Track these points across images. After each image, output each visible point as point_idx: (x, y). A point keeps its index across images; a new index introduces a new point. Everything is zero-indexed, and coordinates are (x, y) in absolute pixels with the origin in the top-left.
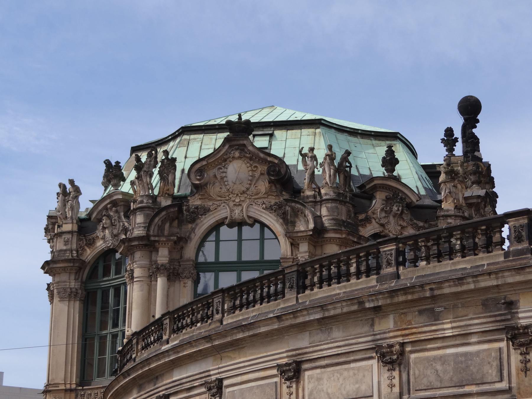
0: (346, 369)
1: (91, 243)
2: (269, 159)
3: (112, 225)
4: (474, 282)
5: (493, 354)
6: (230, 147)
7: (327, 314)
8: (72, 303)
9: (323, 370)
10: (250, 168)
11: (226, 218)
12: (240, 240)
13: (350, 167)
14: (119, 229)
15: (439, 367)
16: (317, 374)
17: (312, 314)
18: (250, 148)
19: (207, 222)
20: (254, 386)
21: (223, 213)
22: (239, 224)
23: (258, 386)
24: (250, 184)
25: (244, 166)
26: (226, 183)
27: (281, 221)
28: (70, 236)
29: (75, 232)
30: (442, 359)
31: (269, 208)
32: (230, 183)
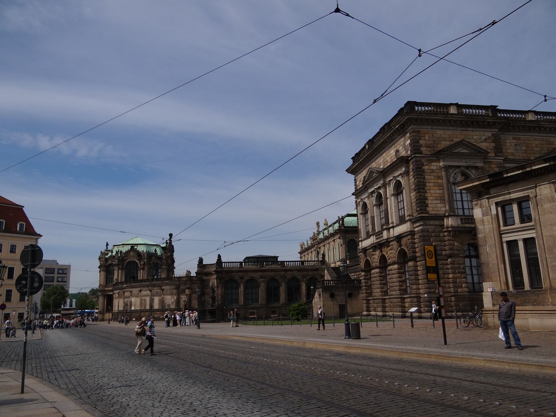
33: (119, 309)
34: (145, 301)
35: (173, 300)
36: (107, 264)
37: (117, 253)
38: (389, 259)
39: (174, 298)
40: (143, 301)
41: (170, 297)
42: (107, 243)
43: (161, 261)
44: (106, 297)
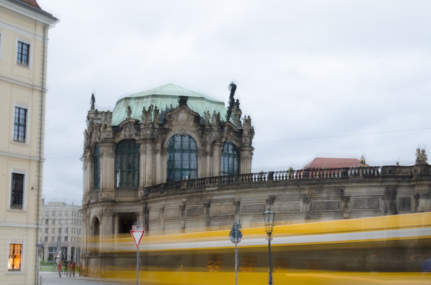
0: (291, 203)
3: (129, 131)
4: (334, 185)
5: (337, 202)
6: (180, 108)
7: (286, 188)
8: (111, 159)
9: (282, 202)
11: (178, 134)
13: (220, 118)
14: (133, 132)
15: (321, 205)
16: (280, 203)
17: (281, 187)
20: (254, 205)
23: (256, 205)
24: (187, 122)
25: (185, 116)
26: (178, 121)
28: (109, 133)
29: (111, 131)
30: (323, 202)
32: (180, 121)
36: (117, 140)
37: (146, 113)
38: (408, 173)
42: (93, 96)
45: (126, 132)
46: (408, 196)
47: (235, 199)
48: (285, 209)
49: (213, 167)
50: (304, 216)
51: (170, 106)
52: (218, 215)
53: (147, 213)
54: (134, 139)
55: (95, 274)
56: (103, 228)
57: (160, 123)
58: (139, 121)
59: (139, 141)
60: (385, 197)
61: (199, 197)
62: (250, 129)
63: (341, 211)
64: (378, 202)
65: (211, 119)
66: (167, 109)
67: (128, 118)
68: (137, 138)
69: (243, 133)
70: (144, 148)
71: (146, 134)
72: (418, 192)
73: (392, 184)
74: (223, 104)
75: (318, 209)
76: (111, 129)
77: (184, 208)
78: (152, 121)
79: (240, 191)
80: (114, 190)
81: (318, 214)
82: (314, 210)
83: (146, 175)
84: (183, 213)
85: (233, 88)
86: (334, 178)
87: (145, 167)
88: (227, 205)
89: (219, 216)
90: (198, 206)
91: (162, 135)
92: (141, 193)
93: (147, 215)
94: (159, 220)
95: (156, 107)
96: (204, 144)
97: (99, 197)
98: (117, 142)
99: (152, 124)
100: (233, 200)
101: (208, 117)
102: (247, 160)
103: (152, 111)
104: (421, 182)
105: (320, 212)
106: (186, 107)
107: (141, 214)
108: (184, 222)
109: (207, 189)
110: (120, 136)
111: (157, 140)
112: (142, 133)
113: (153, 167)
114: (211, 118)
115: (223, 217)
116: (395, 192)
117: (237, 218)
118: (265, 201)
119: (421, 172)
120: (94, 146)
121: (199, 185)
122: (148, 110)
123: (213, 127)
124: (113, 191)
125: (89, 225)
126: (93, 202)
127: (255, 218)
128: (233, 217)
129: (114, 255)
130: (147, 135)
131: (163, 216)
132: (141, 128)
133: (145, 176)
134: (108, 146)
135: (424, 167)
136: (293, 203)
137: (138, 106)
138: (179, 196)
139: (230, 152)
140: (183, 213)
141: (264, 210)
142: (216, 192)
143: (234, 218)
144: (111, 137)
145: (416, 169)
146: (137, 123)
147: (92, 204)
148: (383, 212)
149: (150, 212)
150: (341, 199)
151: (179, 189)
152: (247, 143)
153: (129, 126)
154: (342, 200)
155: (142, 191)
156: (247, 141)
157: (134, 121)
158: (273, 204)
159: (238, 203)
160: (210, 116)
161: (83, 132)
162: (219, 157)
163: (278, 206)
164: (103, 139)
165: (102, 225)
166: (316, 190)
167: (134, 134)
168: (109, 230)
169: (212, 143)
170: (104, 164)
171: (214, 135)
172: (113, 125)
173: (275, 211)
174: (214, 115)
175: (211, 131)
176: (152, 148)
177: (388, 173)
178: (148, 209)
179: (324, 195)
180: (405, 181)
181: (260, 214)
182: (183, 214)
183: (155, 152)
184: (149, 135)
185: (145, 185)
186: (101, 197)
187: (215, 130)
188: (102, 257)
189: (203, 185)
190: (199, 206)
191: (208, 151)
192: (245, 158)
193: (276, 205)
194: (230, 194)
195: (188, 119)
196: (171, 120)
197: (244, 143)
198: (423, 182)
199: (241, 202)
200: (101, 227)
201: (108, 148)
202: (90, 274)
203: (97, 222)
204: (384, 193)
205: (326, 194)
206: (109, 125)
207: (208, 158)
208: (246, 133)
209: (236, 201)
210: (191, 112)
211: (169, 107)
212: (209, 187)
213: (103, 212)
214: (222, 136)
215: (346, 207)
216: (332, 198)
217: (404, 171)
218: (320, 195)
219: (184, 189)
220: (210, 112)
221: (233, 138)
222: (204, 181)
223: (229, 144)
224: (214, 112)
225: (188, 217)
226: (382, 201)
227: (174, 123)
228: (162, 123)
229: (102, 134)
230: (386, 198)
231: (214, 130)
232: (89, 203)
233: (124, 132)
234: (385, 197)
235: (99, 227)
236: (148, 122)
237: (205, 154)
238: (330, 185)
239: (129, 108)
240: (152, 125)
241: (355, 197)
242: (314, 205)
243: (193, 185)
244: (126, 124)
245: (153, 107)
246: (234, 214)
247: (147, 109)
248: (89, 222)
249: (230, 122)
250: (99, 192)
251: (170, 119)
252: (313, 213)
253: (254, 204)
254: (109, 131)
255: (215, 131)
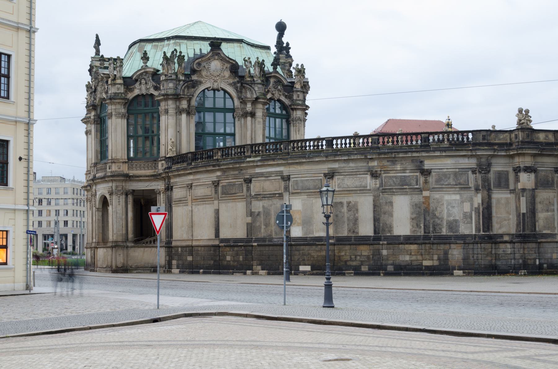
0: (355, 177)
1: (131, 90)
2: (231, 61)
3: (146, 83)
6: (212, 53)
7: (350, 158)
8: (123, 120)
9: (345, 176)
10: (222, 65)
11: (210, 87)
12: (214, 97)
13: (264, 67)
15: (394, 180)
18: (222, 55)
19: (202, 88)
21: (208, 85)
22: (214, 90)
23: (311, 180)
25: (219, 63)
27: (235, 91)
28: (120, 86)
29: (122, 84)
30: (396, 177)
31: (230, 84)
32: (212, 71)
33: (222, 236)
34: (353, 208)
35: (467, 207)
36: (130, 96)
37: (167, 60)
38: (506, 140)
39: (471, 200)
40: (345, 209)
41: (458, 197)
42: (97, 37)
43: (290, 97)
44: (130, 198)
45: (142, 85)
46: (505, 169)
47: (284, 172)
48: (347, 185)
49: (255, 130)
50: (372, 194)
51: (199, 51)
52: (261, 193)
53: (171, 191)
54: (152, 95)
55: (104, 268)
56: (114, 210)
57: (186, 73)
58: (158, 71)
59: (158, 97)
60: (477, 170)
61: (237, 170)
62: (304, 82)
63: (420, 188)
64: (468, 177)
65: (253, 68)
66: (194, 54)
67: (144, 67)
68: (156, 93)
69: (295, 86)
70: (165, 106)
71: (168, 88)
72: (518, 163)
73: (485, 153)
74: (268, 48)
75: (390, 186)
76: (122, 80)
77: (218, 184)
78: (176, 71)
79: (290, 162)
80: (127, 160)
81: (391, 192)
82: (385, 186)
83: (168, 142)
84: (216, 190)
85: (281, 28)
86: (412, 145)
87: (166, 130)
88: (273, 181)
89: (262, 195)
90: (236, 182)
91: (188, 89)
92: (162, 164)
93: (170, 193)
94: (186, 199)
95: (181, 52)
96: (243, 102)
97: (108, 170)
98: (131, 98)
99: (176, 74)
100: (280, 173)
101: (249, 65)
102: (299, 121)
103: (176, 58)
104: (523, 151)
105: (392, 189)
106: (220, 52)
107: (163, 191)
108: (219, 202)
109: (248, 159)
110: (133, 90)
111: (182, 96)
112: (163, 86)
113: (178, 131)
114: (252, 67)
115: (268, 196)
116: (489, 163)
117: (286, 196)
118: (322, 175)
119: (523, 139)
120: (100, 104)
121: (238, 154)
122: (170, 57)
123: (255, 79)
124: (126, 162)
125: (95, 206)
126: (99, 176)
127: (309, 196)
128: (281, 196)
129: (128, 245)
130: (169, 89)
131: (191, 194)
132: (161, 79)
133: (168, 143)
134: (119, 103)
135: (527, 132)
136: (359, 177)
137: (158, 50)
138: (211, 168)
139: (277, 112)
140: (216, 190)
141: (320, 187)
142: (259, 164)
143: (283, 197)
144: (122, 91)
145: (517, 135)
146: (155, 74)
147: (98, 179)
148: (473, 189)
149: (174, 190)
150: (420, 172)
151: (212, 159)
152: (300, 100)
153: (145, 77)
154: (421, 174)
155: (163, 162)
156: (300, 97)
157: (152, 70)
158: (332, 178)
159: (288, 178)
160: (251, 64)
161: (85, 85)
162: (263, 118)
163: (339, 182)
164: (112, 94)
165: (112, 205)
166: (388, 161)
167: (152, 88)
168: (121, 212)
169: (254, 99)
170: (113, 127)
171: (256, 89)
172: (125, 76)
173: (335, 187)
174: (257, 63)
175: (252, 84)
176: (177, 106)
177: (481, 139)
178: (171, 185)
179: (398, 167)
180: (503, 150)
181: (315, 192)
182: (216, 192)
183: (179, 112)
184: (171, 89)
185: (166, 154)
186: (110, 170)
187: (258, 82)
188: (112, 247)
189: (242, 154)
190: (238, 182)
191: (249, 109)
192: (297, 119)
193: (337, 180)
194: (278, 165)
195: (223, 68)
196: (200, 69)
197: (296, 100)
198: (525, 151)
199: (291, 176)
200: (110, 208)
201: (118, 106)
202: (97, 268)
203: (105, 202)
204: (475, 165)
205: (401, 166)
206: (120, 76)
207: (249, 119)
208: (298, 86)
209: (284, 174)
210: (226, 60)
211: (198, 52)
212: (250, 157)
213: (113, 189)
214: (266, 90)
215: (426, 182)
216: (408, 171)
217: (502, 137)
218: (393, 167)
219: (218, 160)
220: (251, 60)
221: (281, 94)
222: (244, 150)
223: (276, 102)
224: (256, 59)
225: (223, 196)
226: (472, 175)
227: (204, 73)
228: (189, 73)
229: (110, 88)
230: (477, 172)
231: (256, 82)
232: (95, 177)
233: (139, 86)
234: (477, 170)
235: (108, 208)
236: (170, 72)
237: (245, 115)
238: (406, 154)
239: (145, 53)
240: (175, 76)
241: (438, 170)
242: (386, 181)
243: (229, 155)
244: (141, 74)
245: (177, 52)
246: (283, 192)
247: (169, 55)
248: (95, 202)
249: (277, 72)
250: (107, 163)
251: (199, 68)
252: (383, 191)
253: (308, 178)
254: (119, 84)
255: (258, 83)
